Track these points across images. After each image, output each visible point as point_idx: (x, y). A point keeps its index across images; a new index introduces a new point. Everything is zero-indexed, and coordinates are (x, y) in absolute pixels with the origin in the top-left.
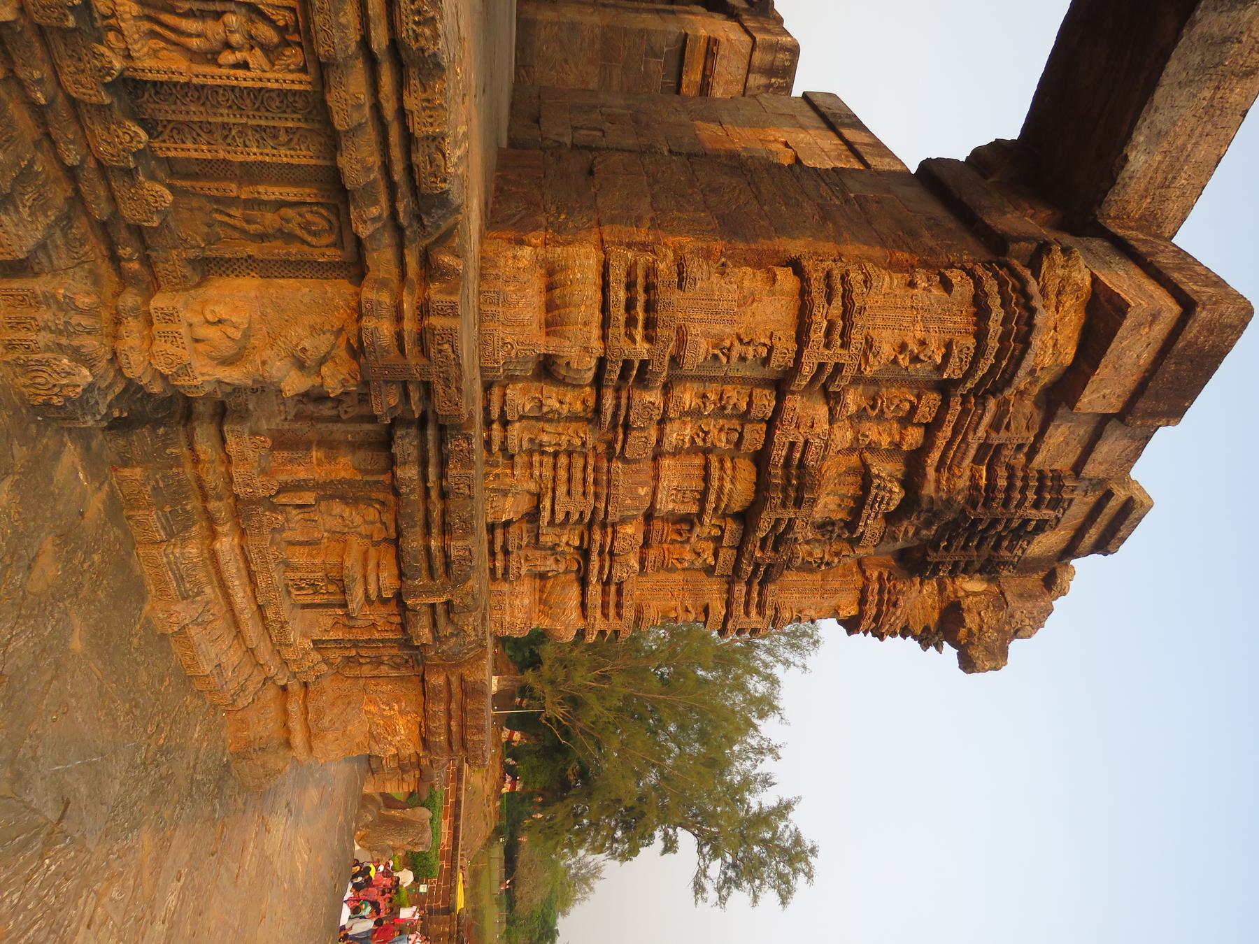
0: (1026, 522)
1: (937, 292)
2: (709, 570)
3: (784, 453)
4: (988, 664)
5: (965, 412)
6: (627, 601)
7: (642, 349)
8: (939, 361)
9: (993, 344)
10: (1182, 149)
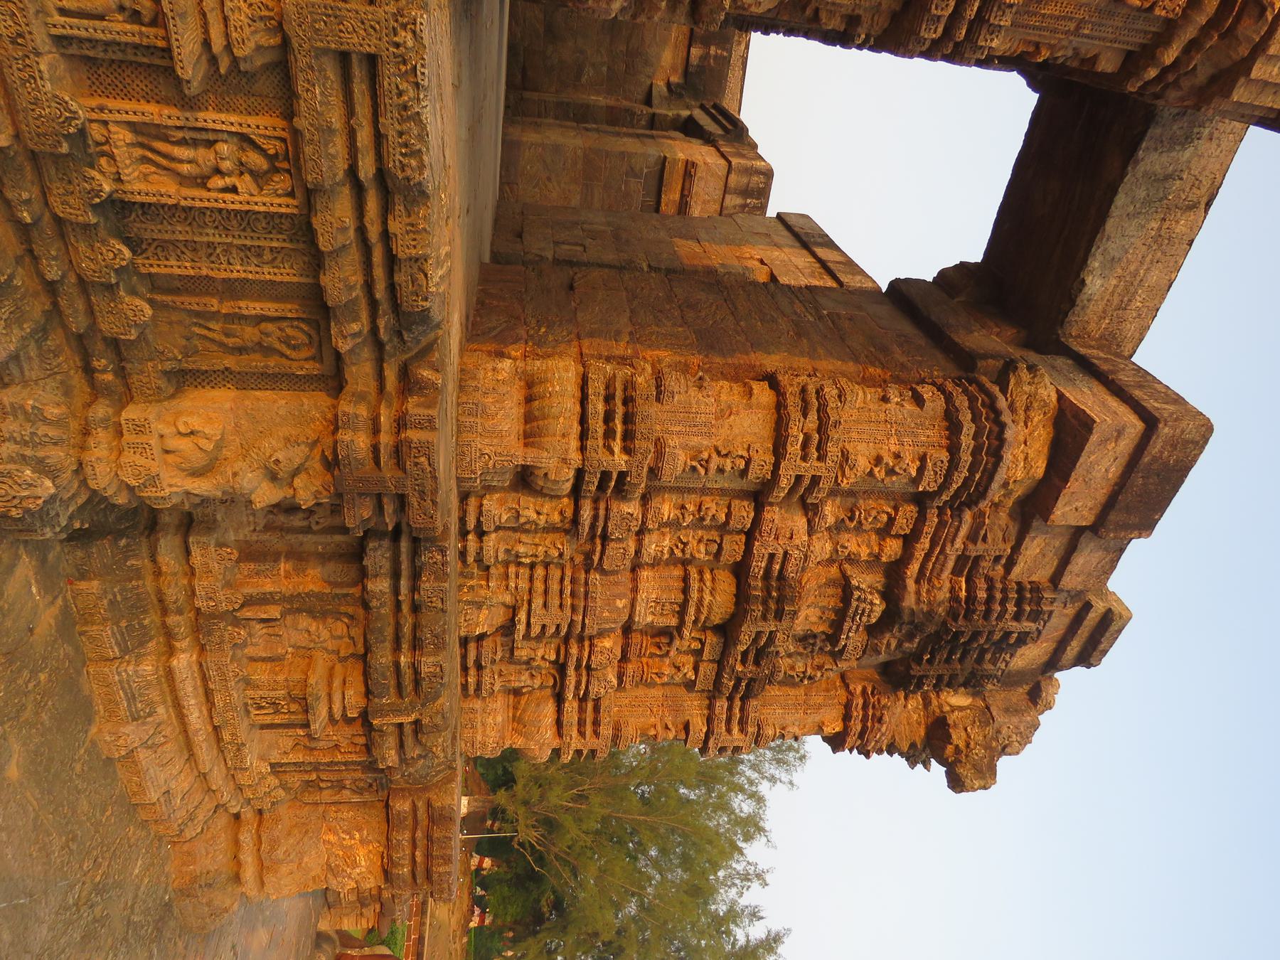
0: (1007, 634)
1: (909, 407)
2: (690, 685)
3: (763, 565)
4: (977, 783)
5: (941, 524)
6: (605, 719)
8: (914, 474)
9: (966, 458)
10: (1135, 274)
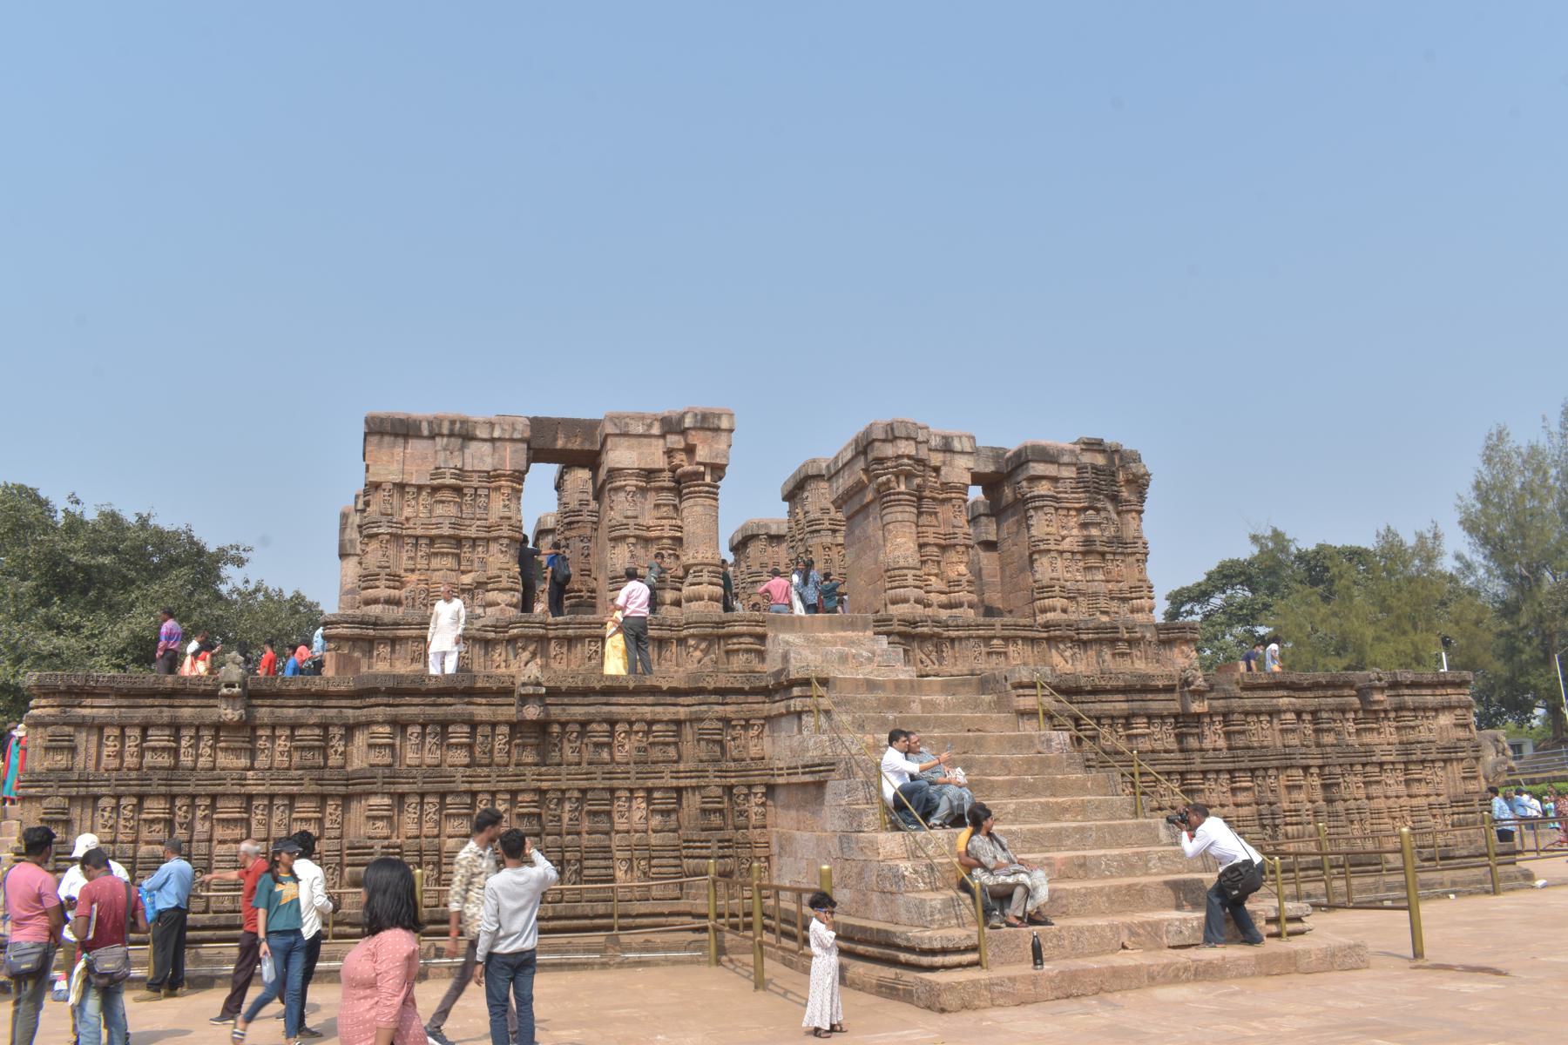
7: (1057, 588)
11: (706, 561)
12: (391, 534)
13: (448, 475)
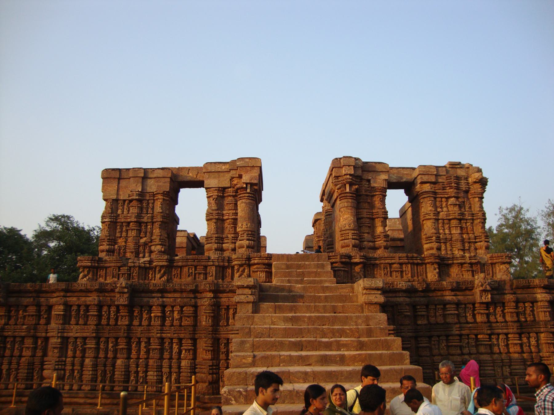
1: (423, 203)
11: (246, 229)
12: (111, 222)
13: (135, 195)
